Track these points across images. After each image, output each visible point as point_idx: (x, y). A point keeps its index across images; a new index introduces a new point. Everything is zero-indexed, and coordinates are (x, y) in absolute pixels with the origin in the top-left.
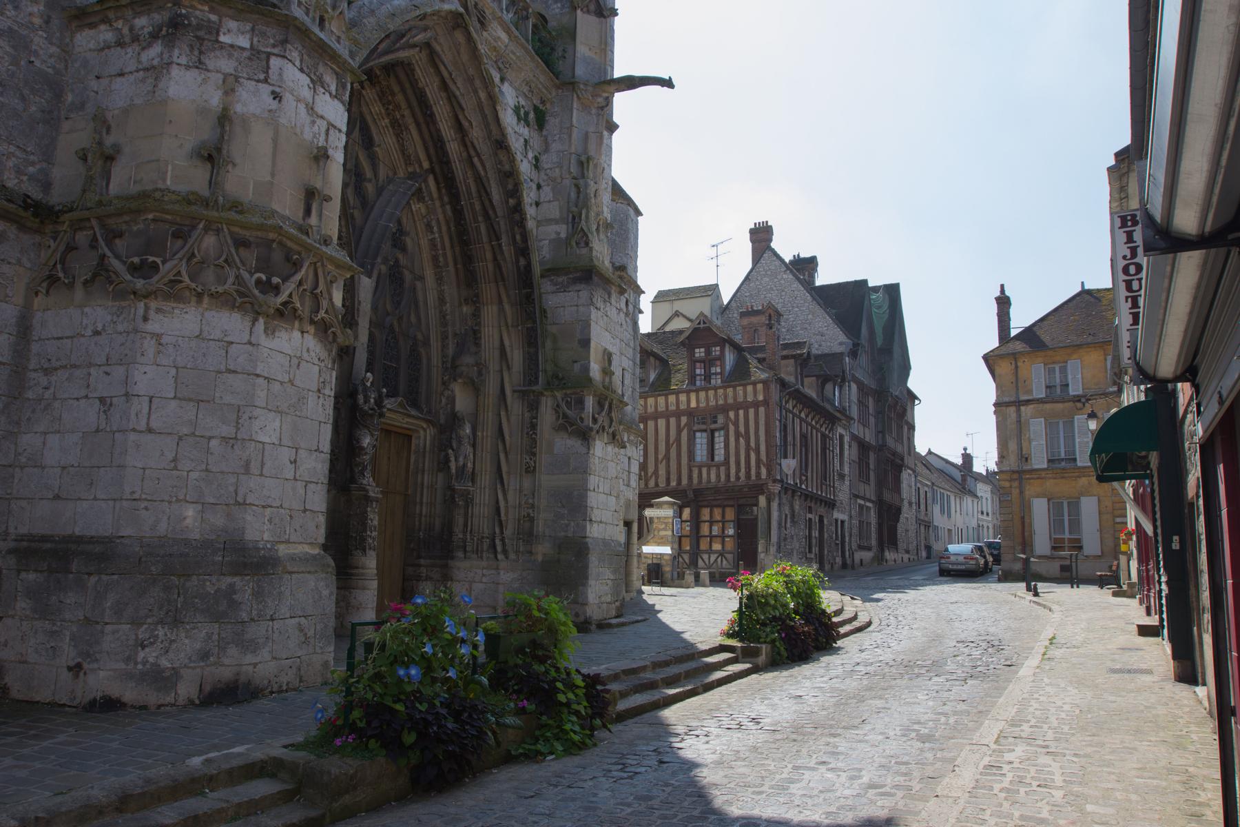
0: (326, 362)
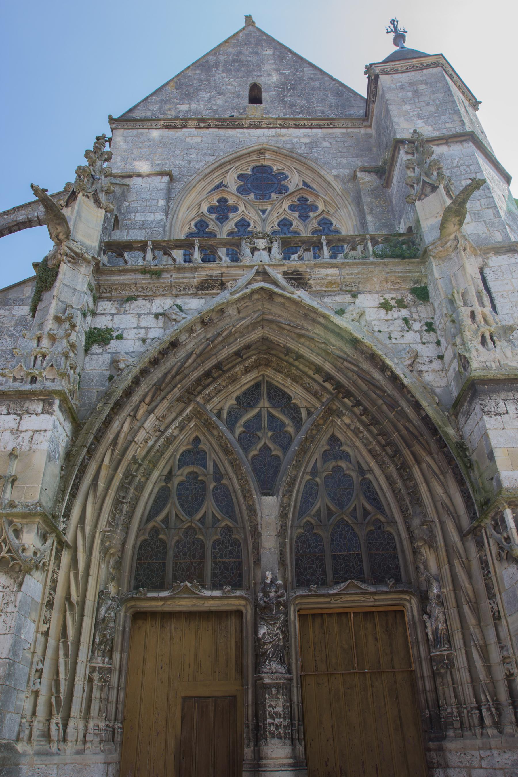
0: (11, 587)
